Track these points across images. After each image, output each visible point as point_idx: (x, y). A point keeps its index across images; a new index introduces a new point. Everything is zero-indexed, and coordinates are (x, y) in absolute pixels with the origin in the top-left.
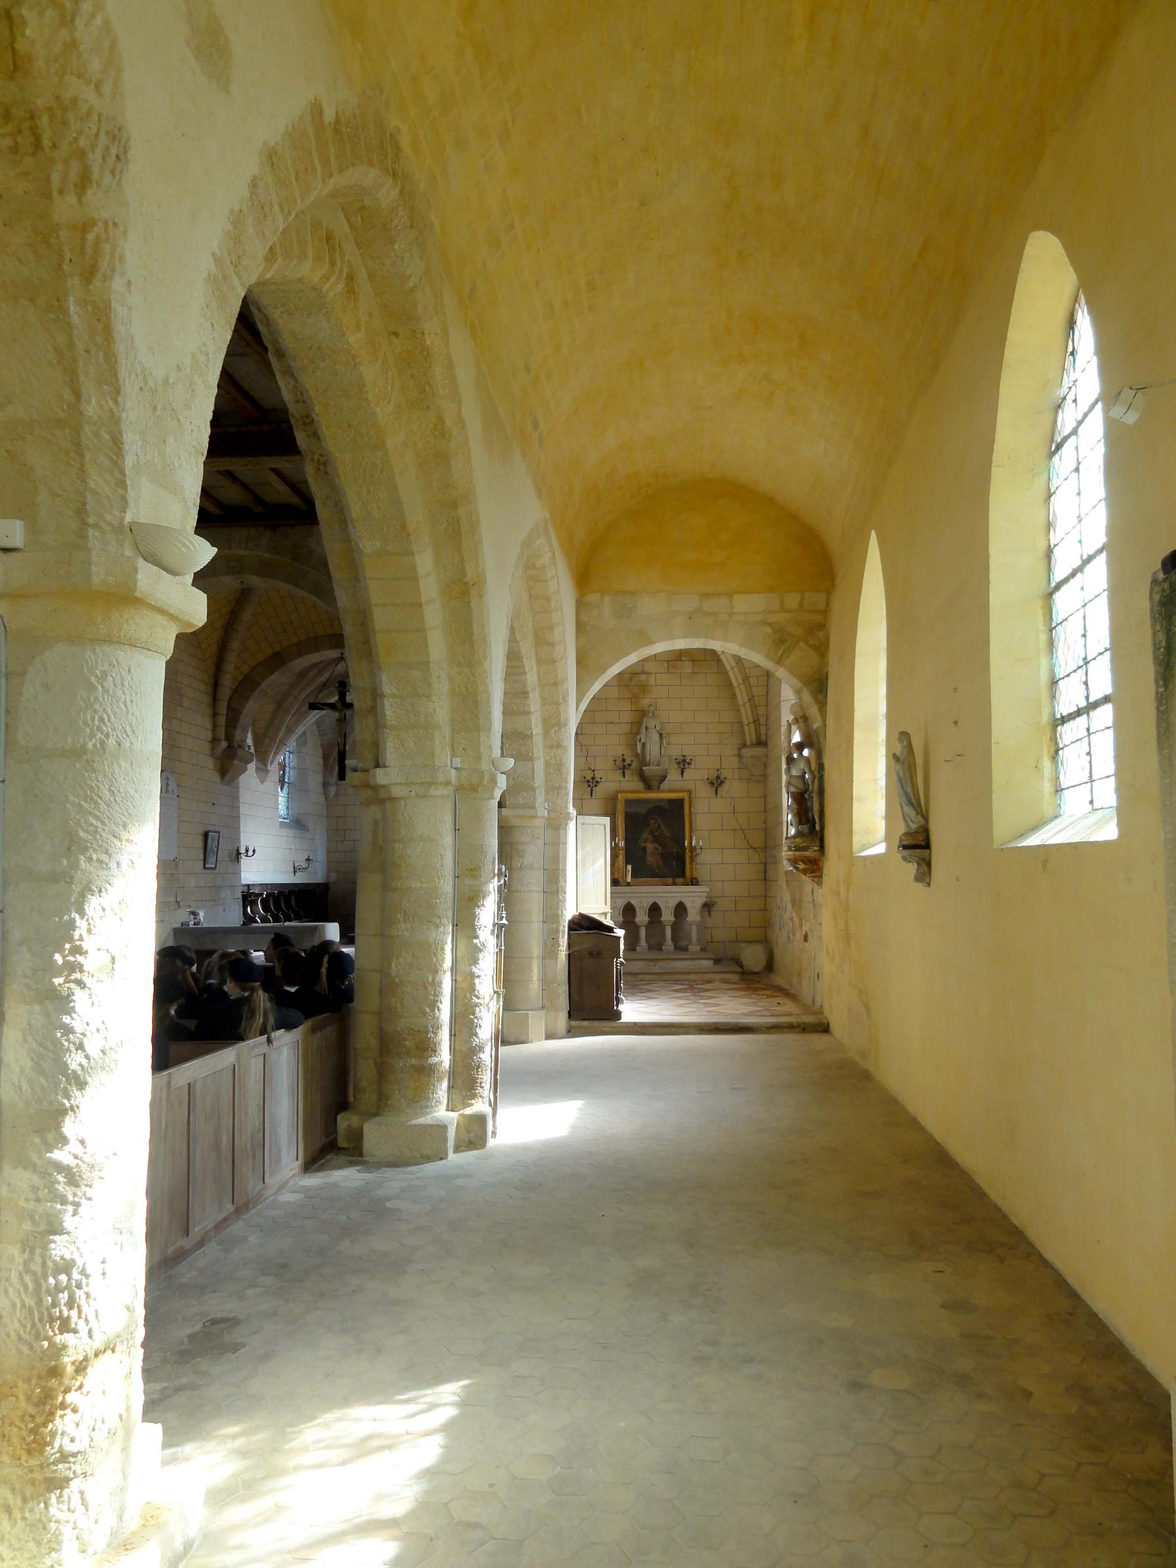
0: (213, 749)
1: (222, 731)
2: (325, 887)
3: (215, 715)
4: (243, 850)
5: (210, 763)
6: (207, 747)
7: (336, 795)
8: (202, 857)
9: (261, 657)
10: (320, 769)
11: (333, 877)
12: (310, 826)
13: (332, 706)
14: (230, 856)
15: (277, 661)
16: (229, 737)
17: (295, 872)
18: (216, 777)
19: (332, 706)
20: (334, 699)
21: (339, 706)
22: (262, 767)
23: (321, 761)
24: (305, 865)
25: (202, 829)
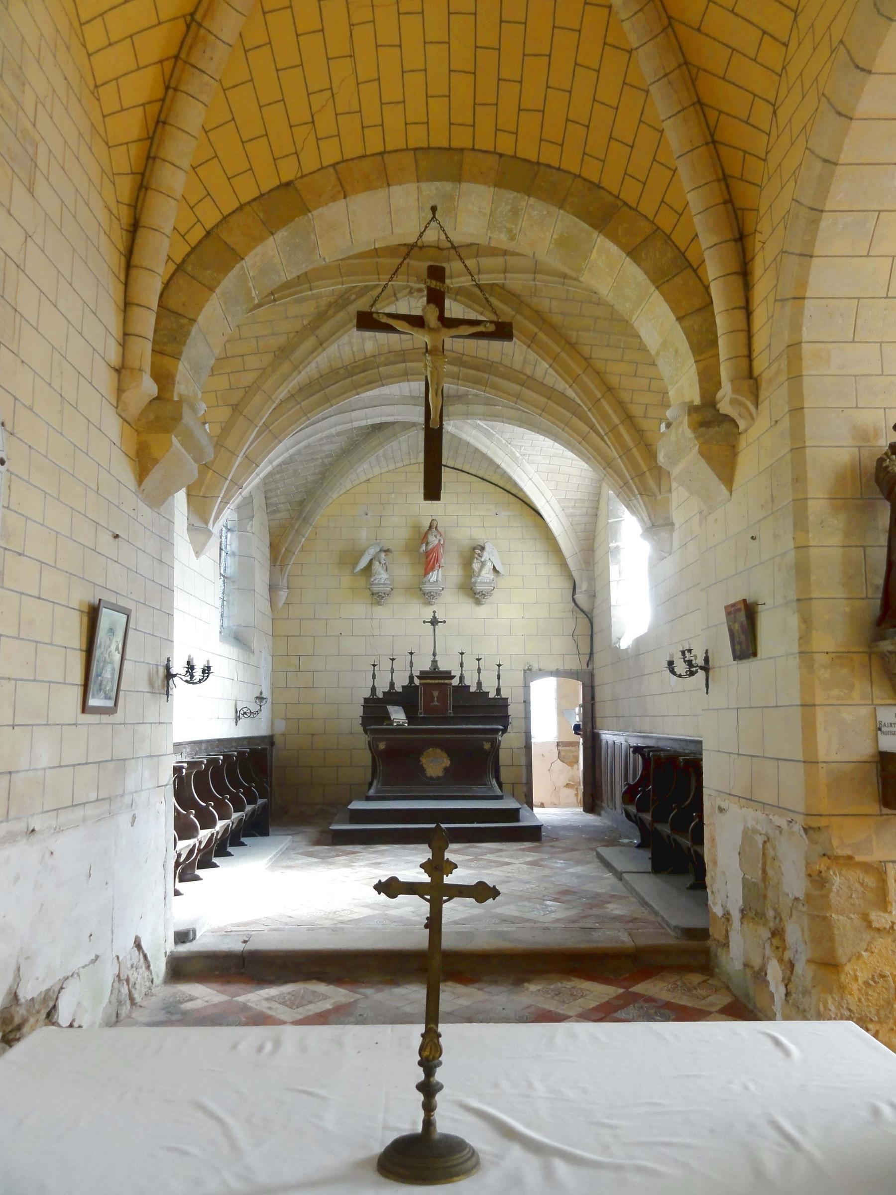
0: (120, 390)
1: (143, 351)
2: (270, 740)
3: (127, 305)
4: (179, 667)
5: (113, 426)
6: (105, 380)
7: (287, 604)
8: (77, 677)
9: (248, 192)
10: (267, 563)
11: (281, 727)
12: (255, 646)
13: (417, 322)
14: (151, 683)
15: (283, 204)
16: (164, 379)
17: (237, 719)
18: (125, 472)
19: (417, 322)
20: (416, 305)
21: (432, 319)
22: (199, 524)
23: (267, 551)
24: (254, 708)
25: (82, 596)
